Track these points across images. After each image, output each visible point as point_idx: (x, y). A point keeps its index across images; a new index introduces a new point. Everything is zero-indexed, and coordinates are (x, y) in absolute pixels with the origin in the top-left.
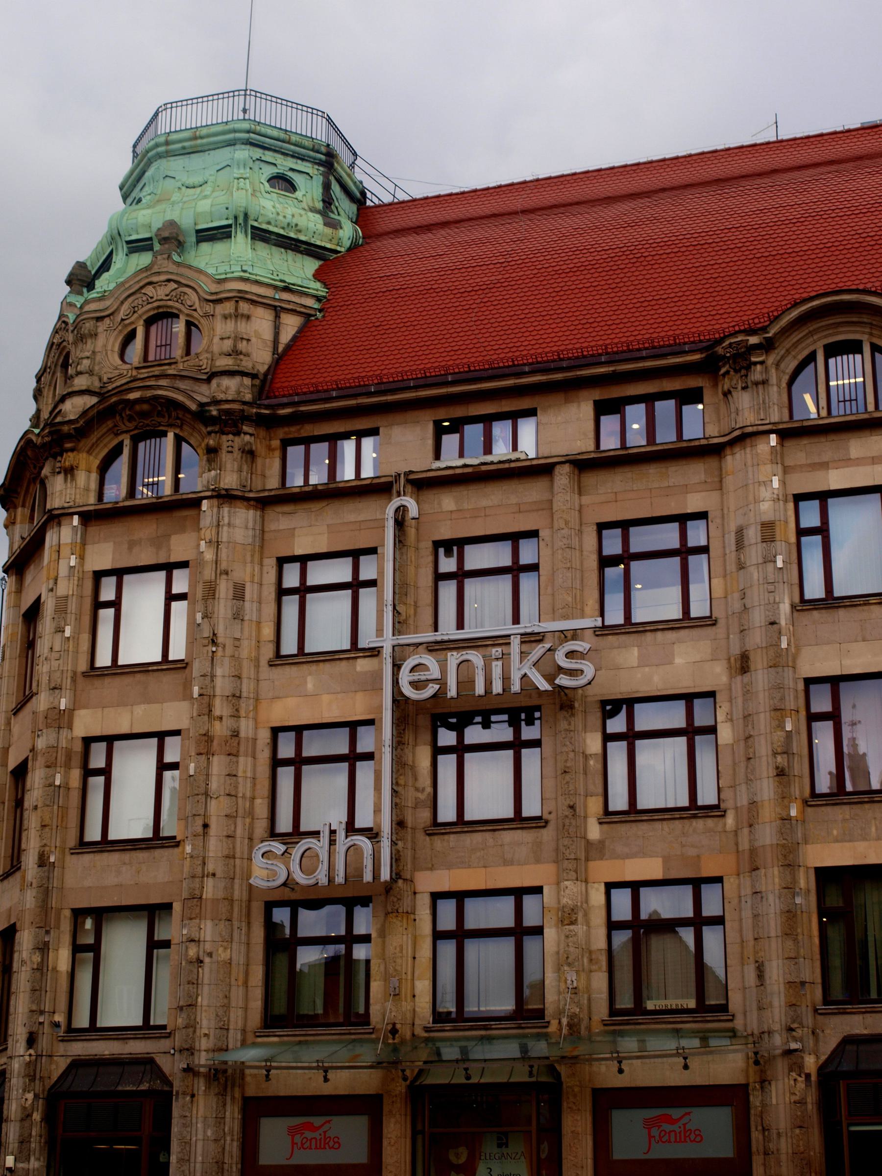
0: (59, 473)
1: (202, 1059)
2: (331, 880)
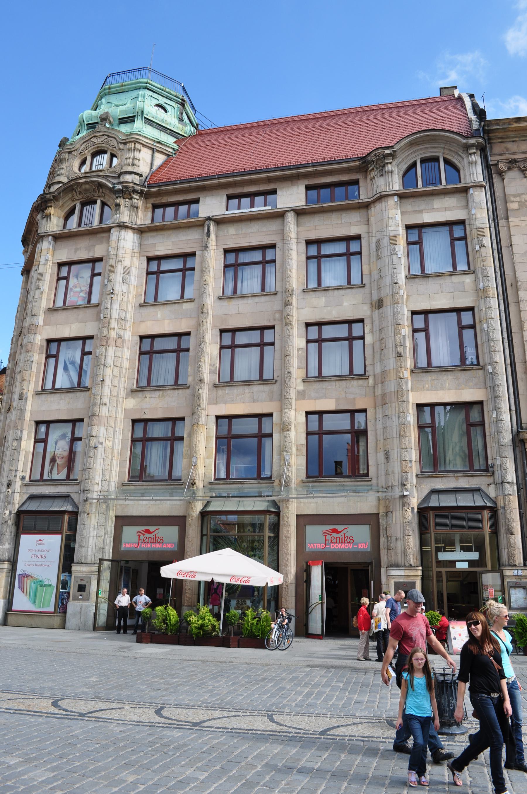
0: (44, 218)
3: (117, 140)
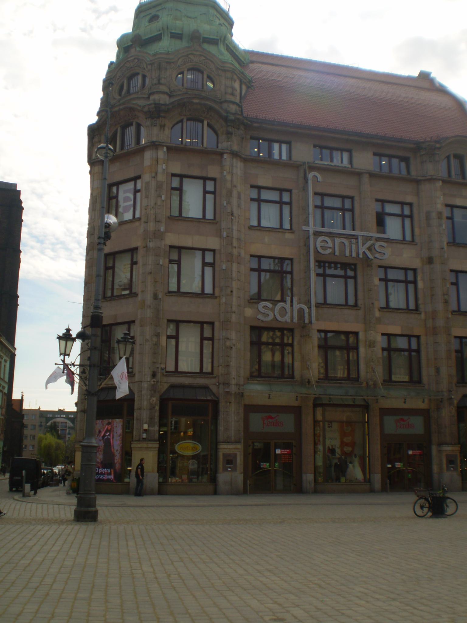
0: (156, 126)
1: (233, 389)
2: (292, 320)
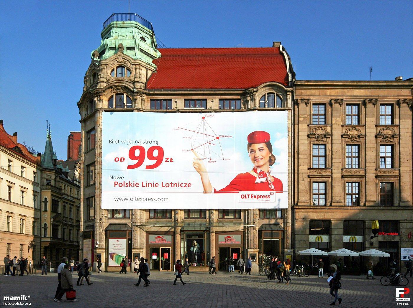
3: (129, 62)
